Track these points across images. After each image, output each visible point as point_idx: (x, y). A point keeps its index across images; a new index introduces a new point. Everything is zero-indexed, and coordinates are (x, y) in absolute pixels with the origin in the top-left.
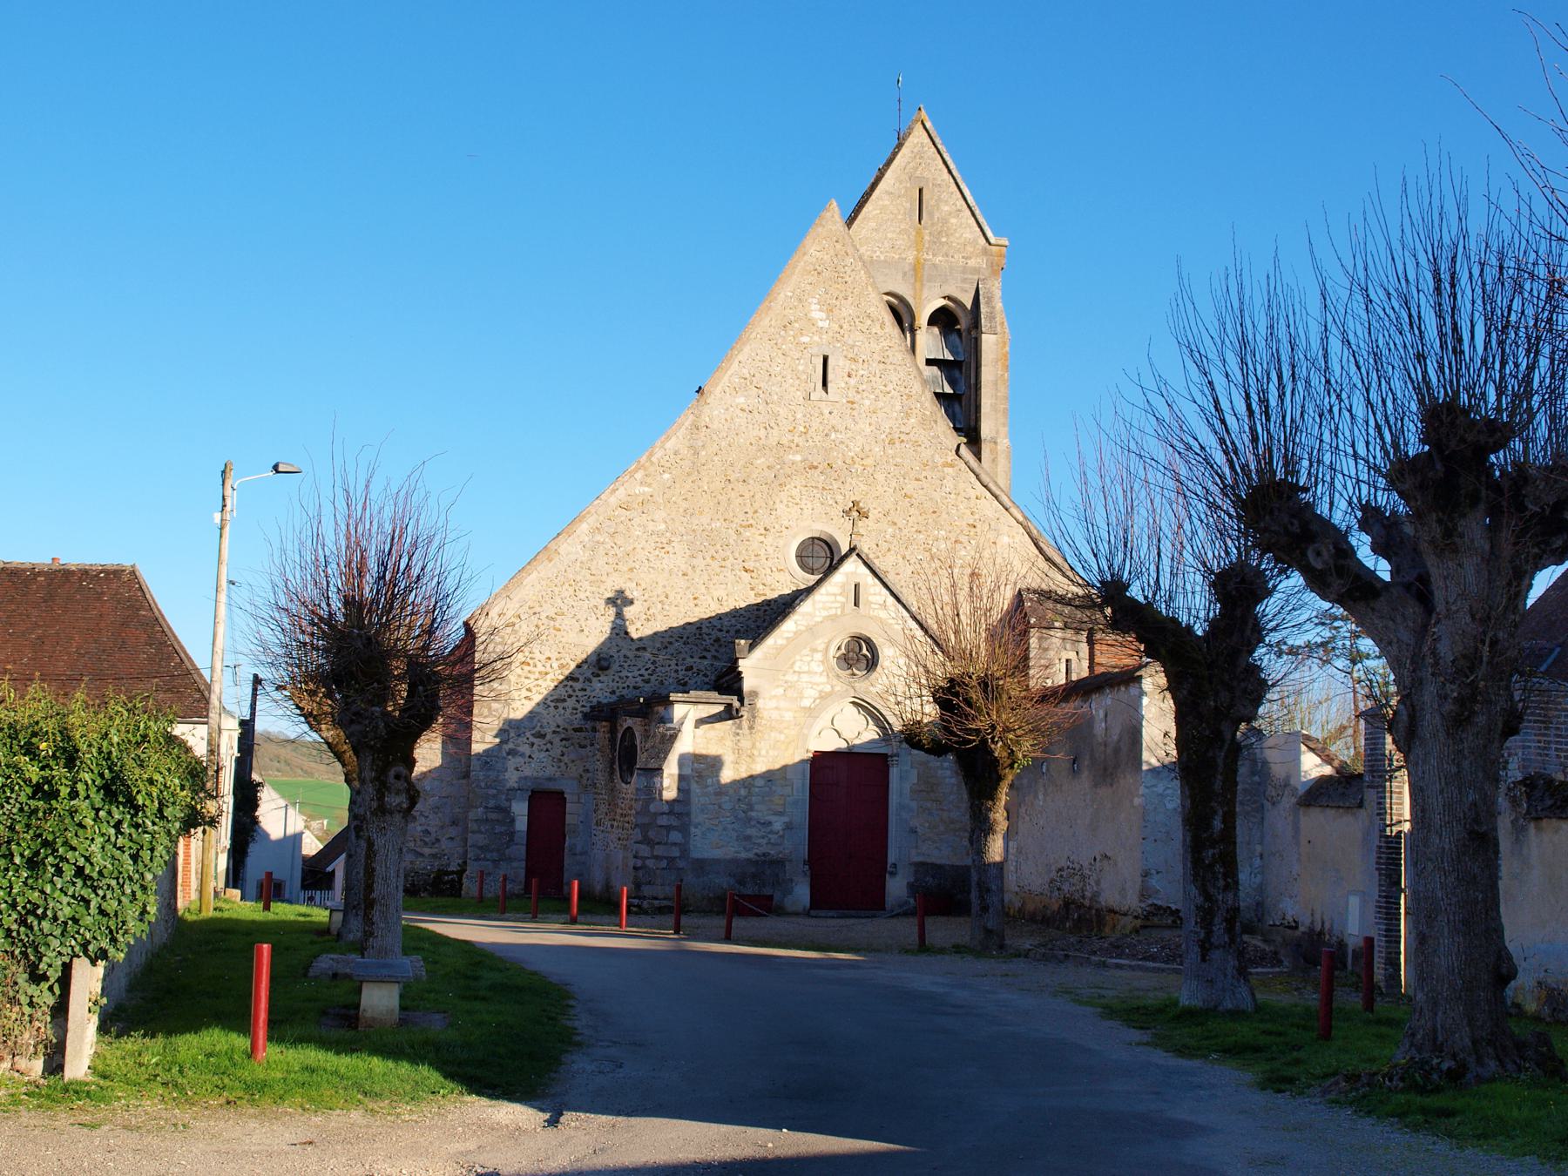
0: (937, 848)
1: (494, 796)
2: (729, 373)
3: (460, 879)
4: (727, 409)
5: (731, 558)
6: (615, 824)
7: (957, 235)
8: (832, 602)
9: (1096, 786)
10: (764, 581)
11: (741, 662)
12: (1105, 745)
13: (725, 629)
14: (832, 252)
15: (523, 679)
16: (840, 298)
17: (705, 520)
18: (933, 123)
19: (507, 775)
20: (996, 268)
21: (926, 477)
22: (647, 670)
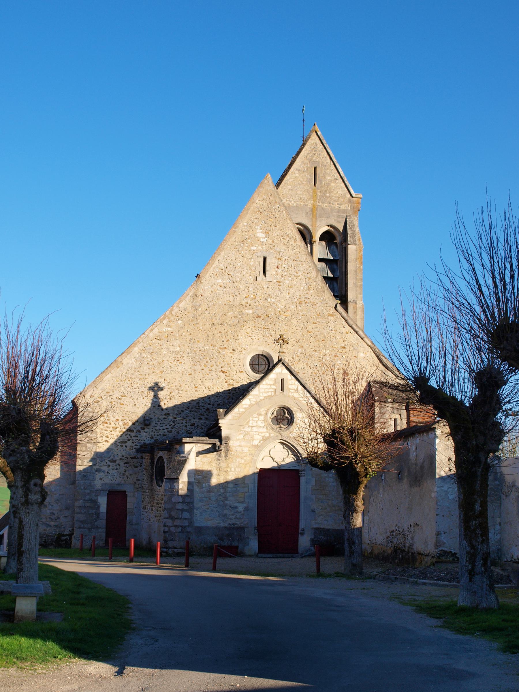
0: (326, 520)
1: (89, 494)
2: (213, 266)
3: (71, 539)
4: (212, 286)
5: (215, 365)
6: (154, 508)
7: (335, 192)
8: (269, 389)
9: (411, 486)
10: (233, 378)
11: (220, 421)
12: (416, 465)
13: (212, 403)
14: (268, 202)
15: (104, 431)
16: (273, 226)
17: (201, 345)
18: (322, 132)
19: (96, 482)
20: (355, 210)
21: (319, 322)
22: (170, 425)
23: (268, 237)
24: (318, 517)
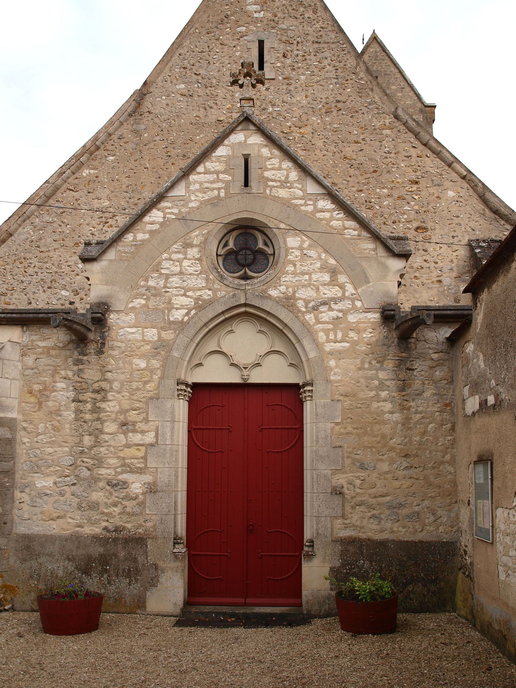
0: (373, 516)
2: (170, 64)
23: (265, 8)
24: (353, 508)
